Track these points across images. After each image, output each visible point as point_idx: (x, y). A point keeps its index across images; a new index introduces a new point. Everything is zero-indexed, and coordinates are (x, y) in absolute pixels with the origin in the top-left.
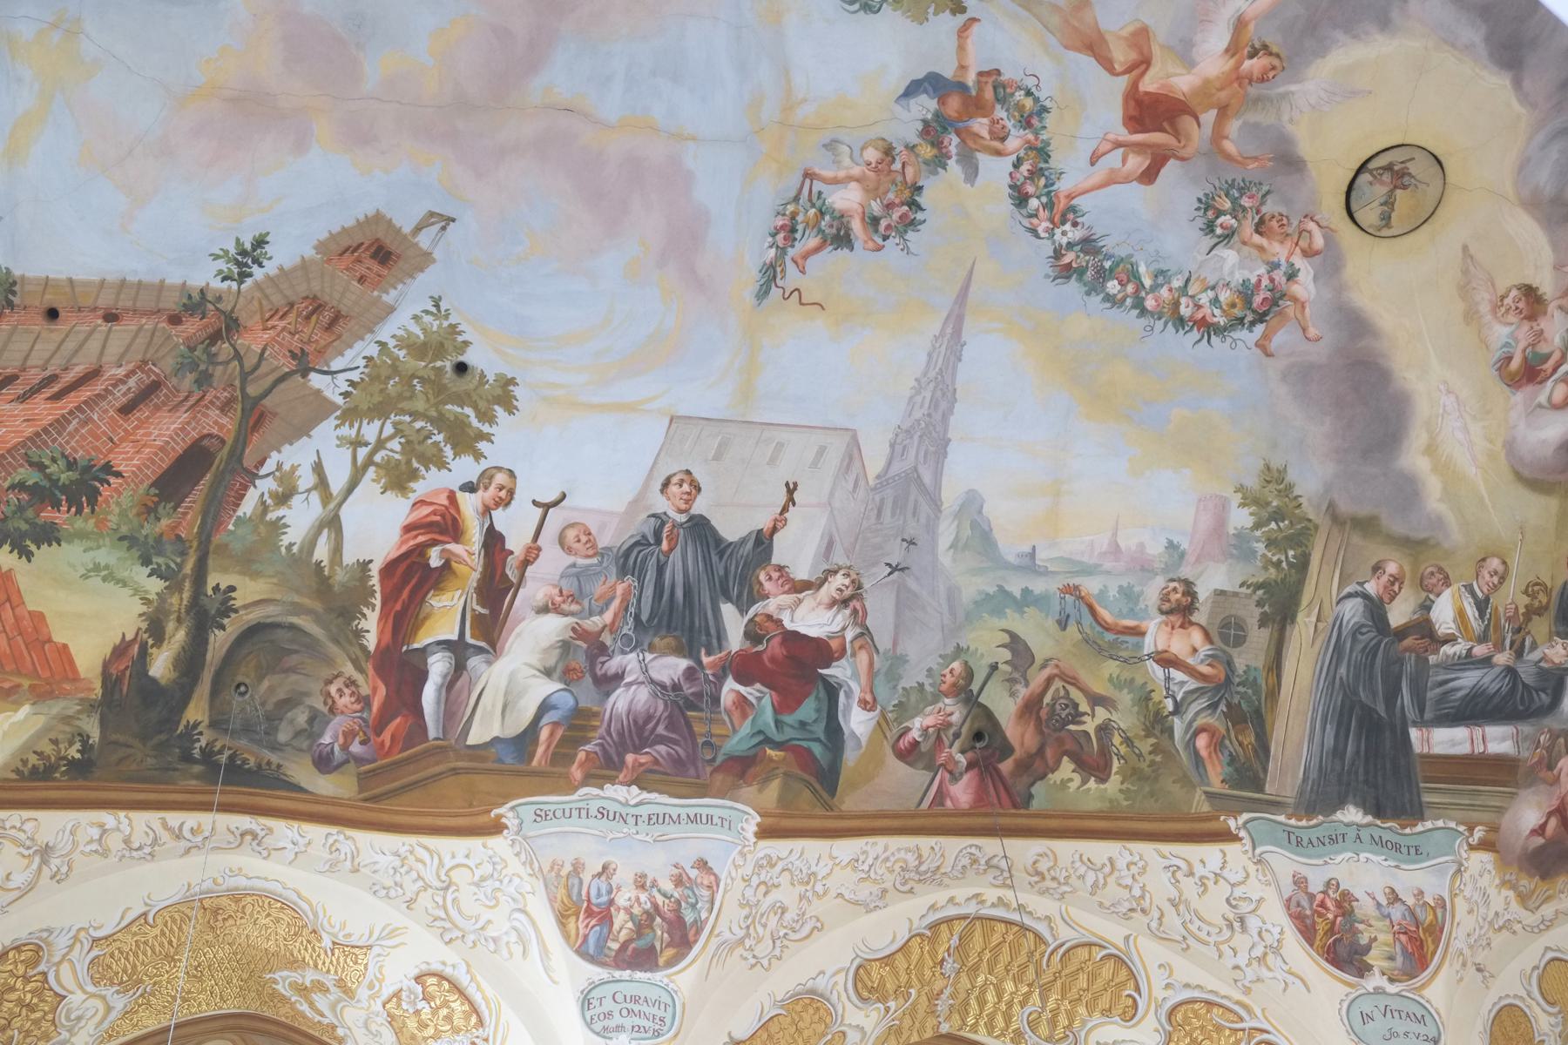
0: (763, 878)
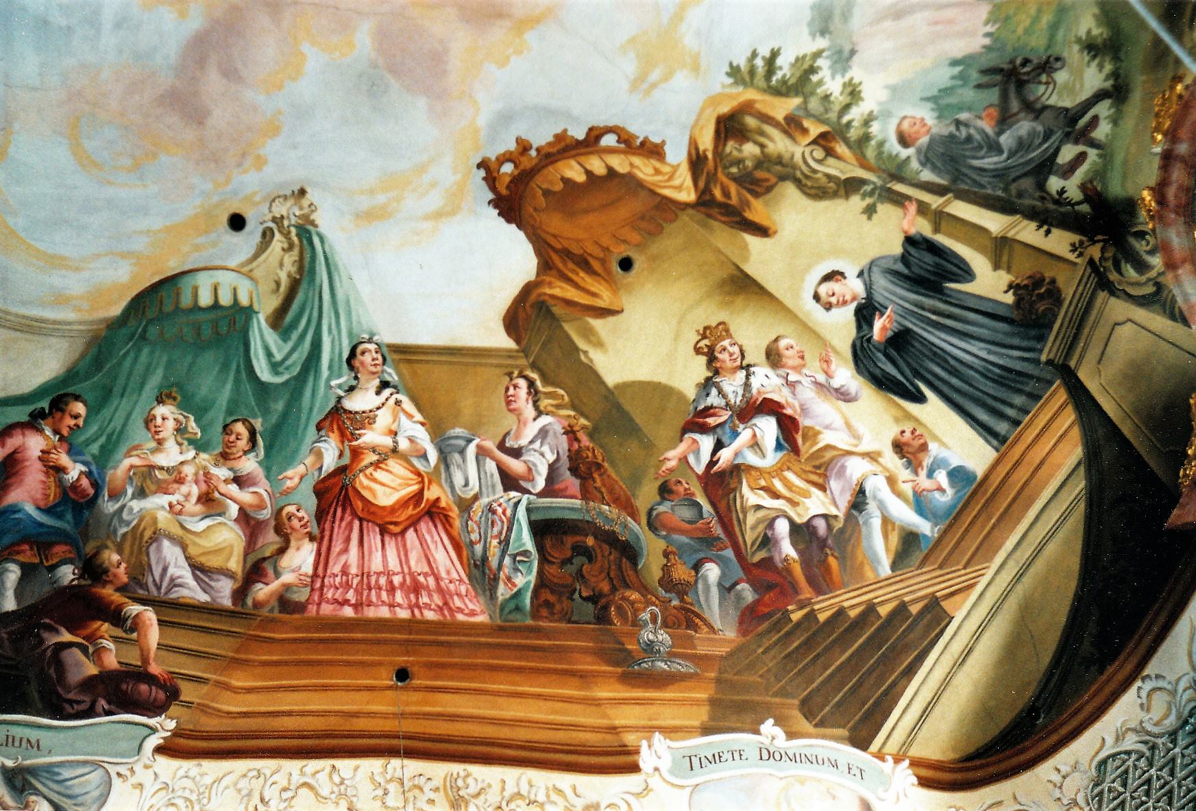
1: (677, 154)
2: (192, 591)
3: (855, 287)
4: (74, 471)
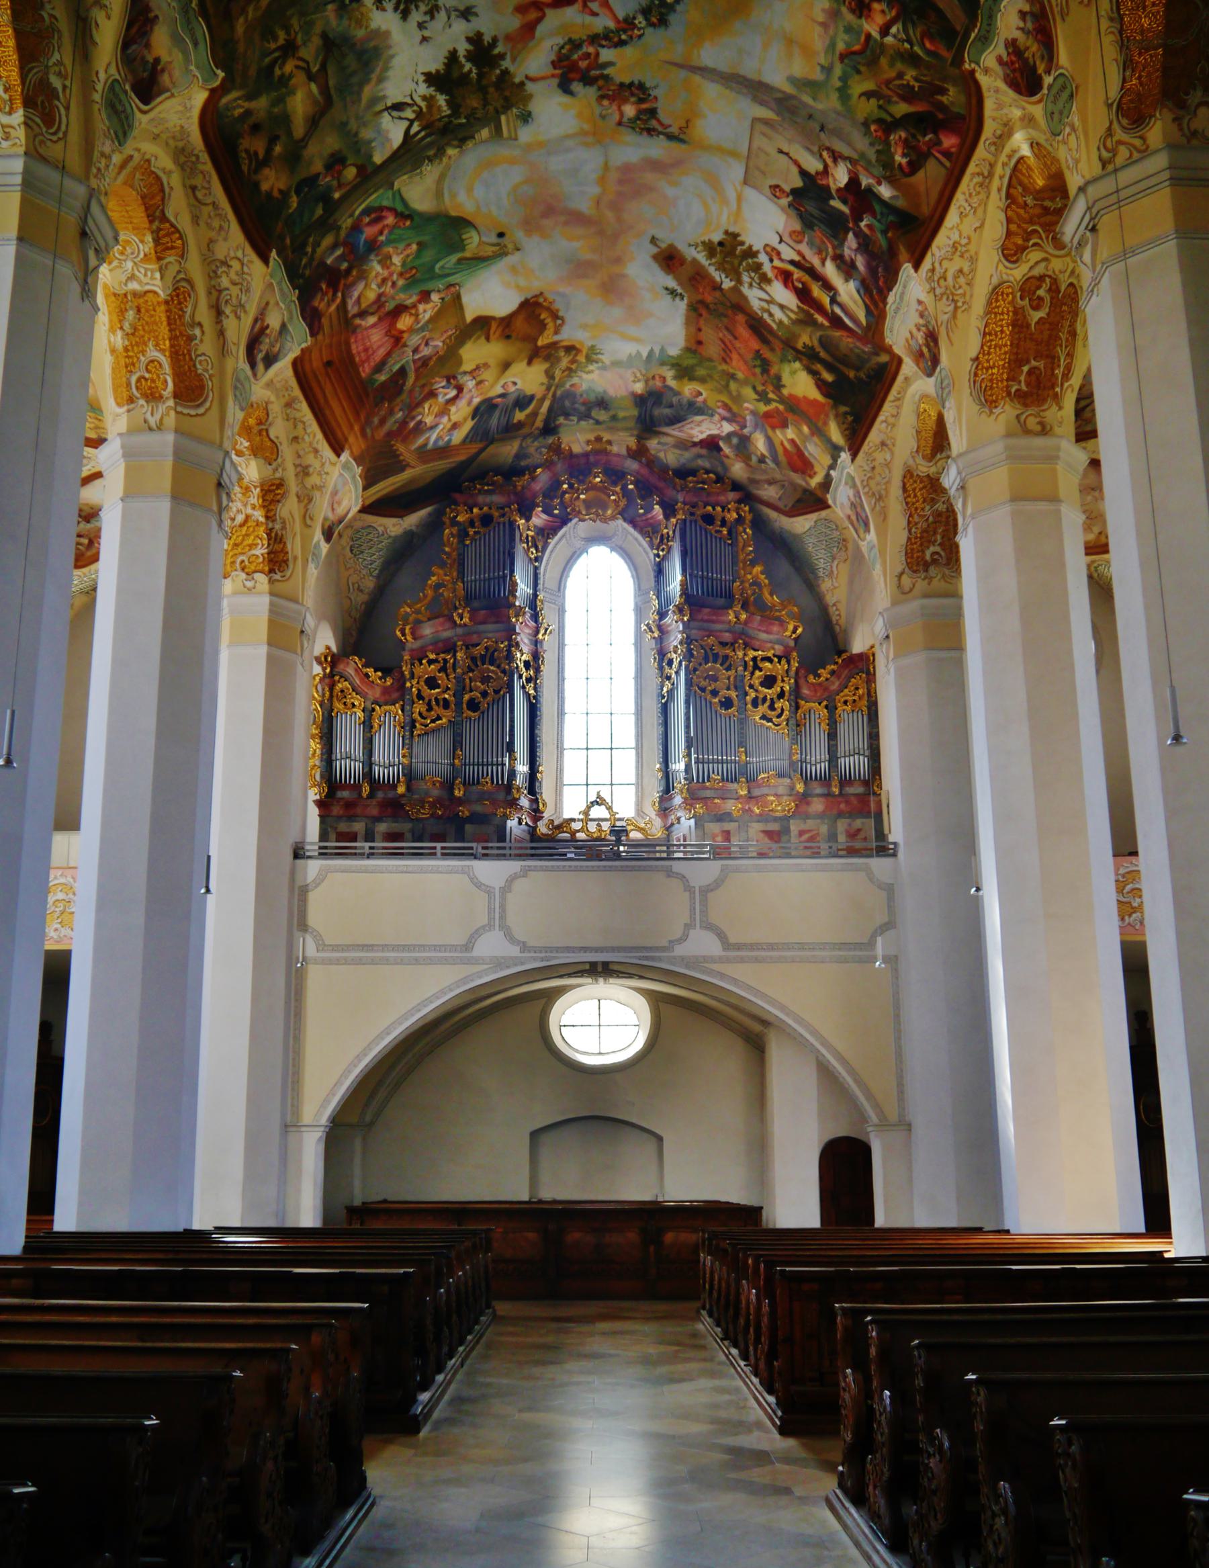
0: (936, 279)
1: (557, 338)
2: (350, 303)
3: (512, 389)
4: (382, 238)
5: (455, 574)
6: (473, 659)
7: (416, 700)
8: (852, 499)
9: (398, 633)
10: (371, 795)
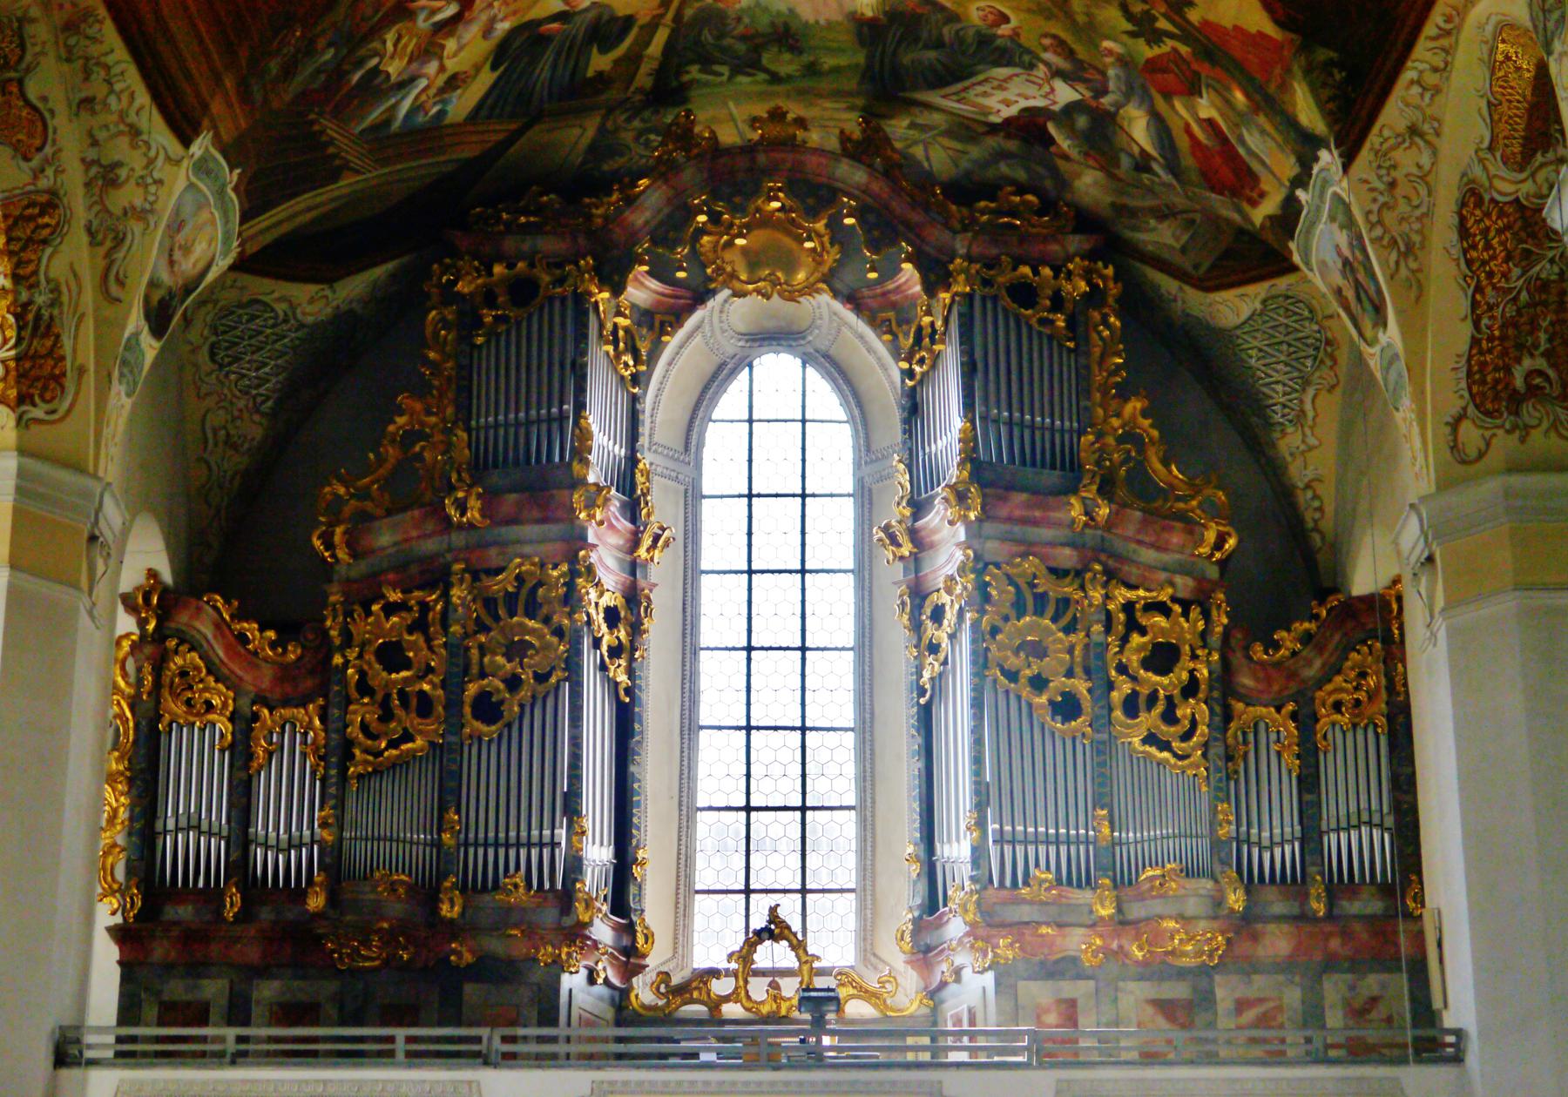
5: (450, 411)
6: (490, 603)
7: (354, 694)
8: (1347, 252)
9: (317, 543)
10: (245, 915)
